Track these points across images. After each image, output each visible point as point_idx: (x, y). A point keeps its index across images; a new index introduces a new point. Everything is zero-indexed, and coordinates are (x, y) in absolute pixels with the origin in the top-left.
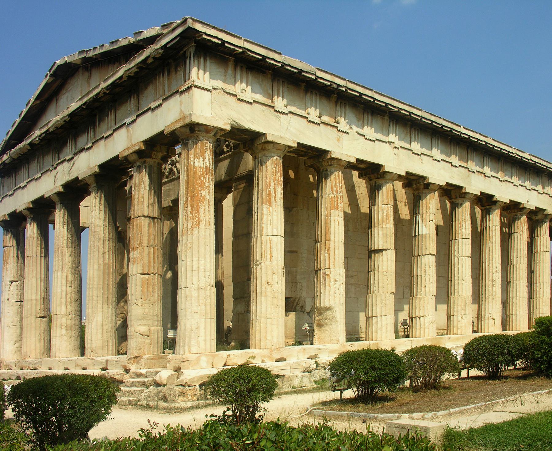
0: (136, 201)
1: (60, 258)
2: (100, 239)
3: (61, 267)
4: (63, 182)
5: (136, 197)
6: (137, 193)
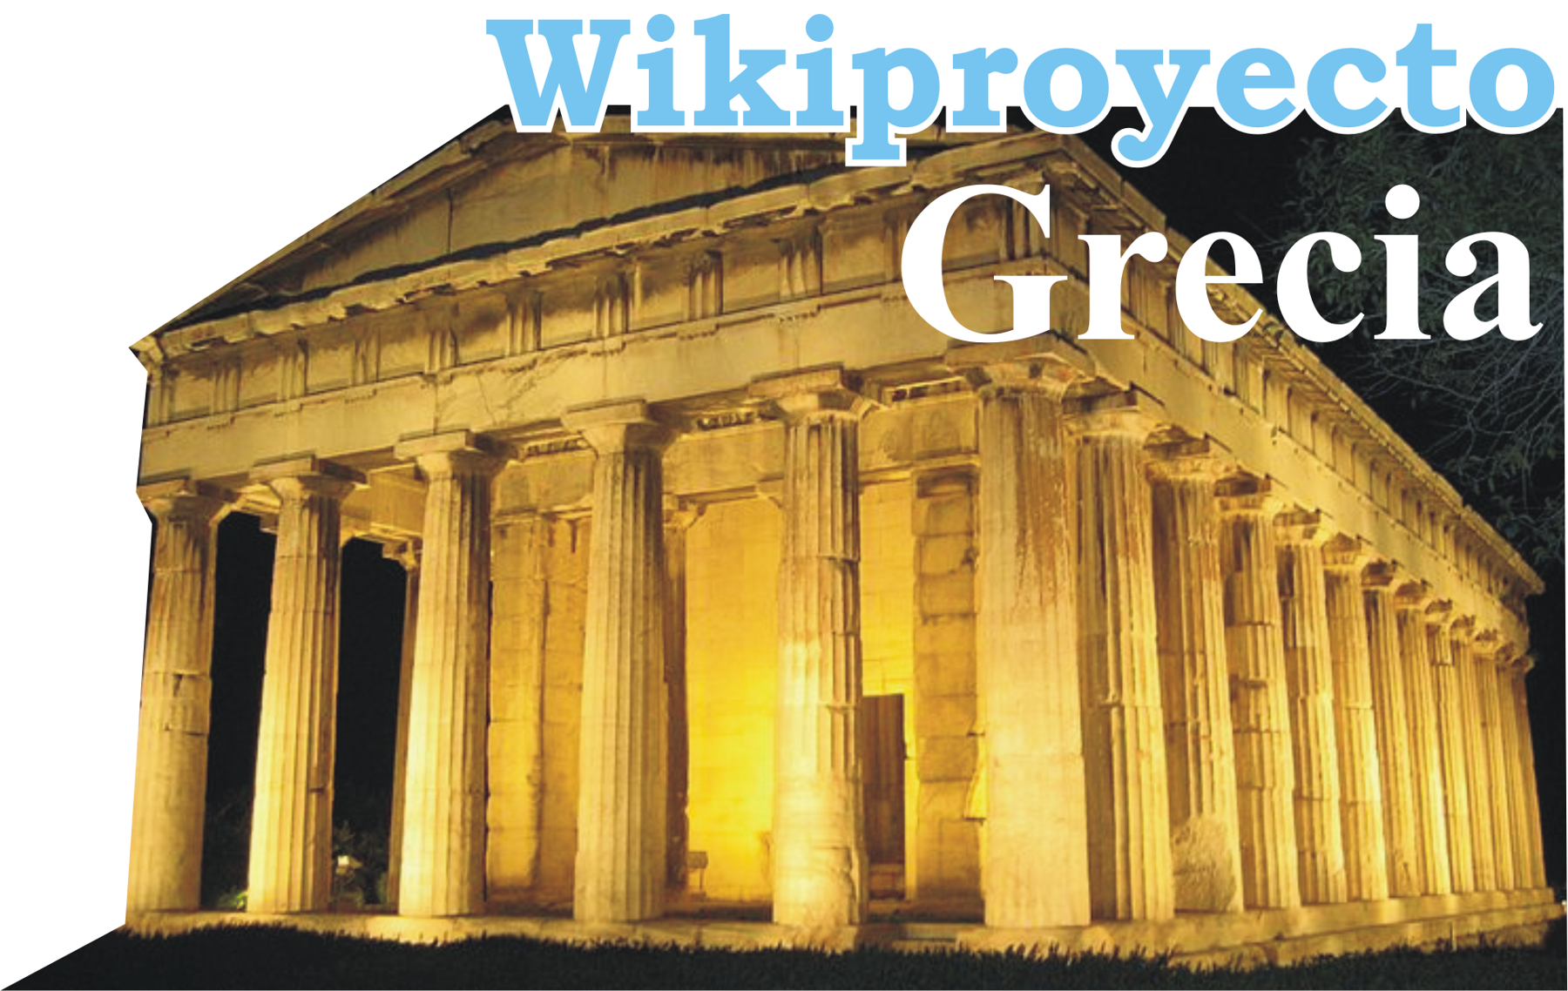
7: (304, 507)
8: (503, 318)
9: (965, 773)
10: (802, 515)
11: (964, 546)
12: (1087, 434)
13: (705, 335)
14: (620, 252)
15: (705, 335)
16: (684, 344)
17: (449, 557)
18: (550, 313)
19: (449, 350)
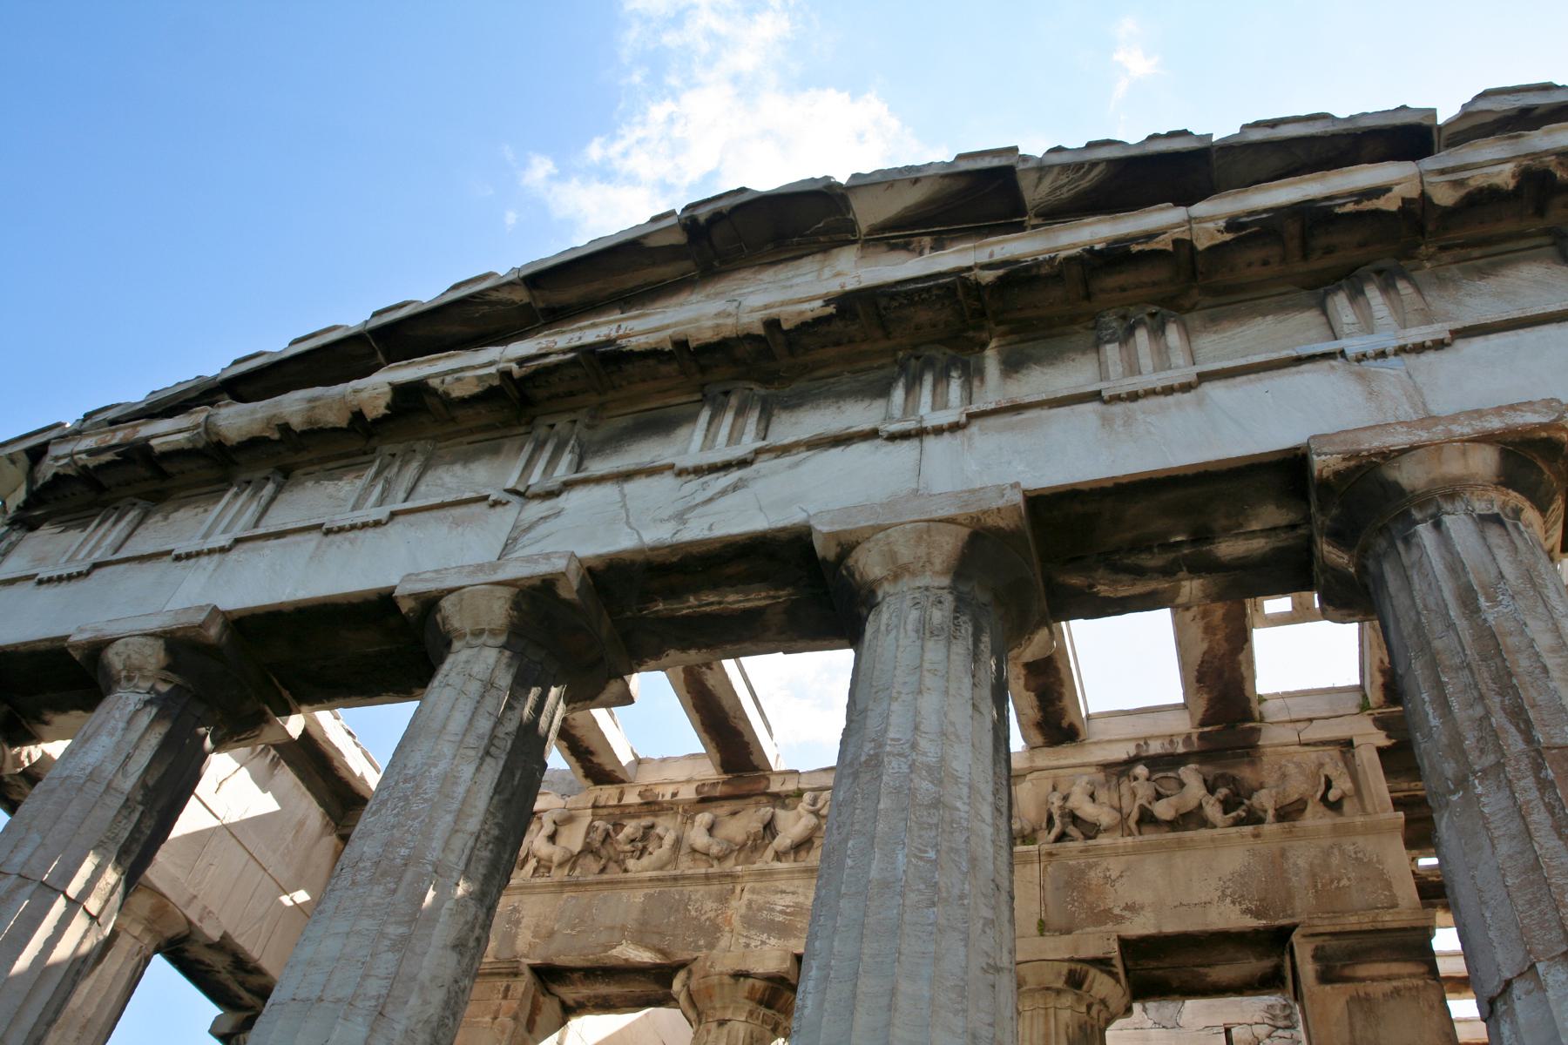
1: (394, 930)
2: (973, 861)
3: (374, 987)
8: (692, 418)
10: (1523, 663)
14: (988, 276)
15: (1168, 391)
16: (1118, 408)
17: (449, 779)
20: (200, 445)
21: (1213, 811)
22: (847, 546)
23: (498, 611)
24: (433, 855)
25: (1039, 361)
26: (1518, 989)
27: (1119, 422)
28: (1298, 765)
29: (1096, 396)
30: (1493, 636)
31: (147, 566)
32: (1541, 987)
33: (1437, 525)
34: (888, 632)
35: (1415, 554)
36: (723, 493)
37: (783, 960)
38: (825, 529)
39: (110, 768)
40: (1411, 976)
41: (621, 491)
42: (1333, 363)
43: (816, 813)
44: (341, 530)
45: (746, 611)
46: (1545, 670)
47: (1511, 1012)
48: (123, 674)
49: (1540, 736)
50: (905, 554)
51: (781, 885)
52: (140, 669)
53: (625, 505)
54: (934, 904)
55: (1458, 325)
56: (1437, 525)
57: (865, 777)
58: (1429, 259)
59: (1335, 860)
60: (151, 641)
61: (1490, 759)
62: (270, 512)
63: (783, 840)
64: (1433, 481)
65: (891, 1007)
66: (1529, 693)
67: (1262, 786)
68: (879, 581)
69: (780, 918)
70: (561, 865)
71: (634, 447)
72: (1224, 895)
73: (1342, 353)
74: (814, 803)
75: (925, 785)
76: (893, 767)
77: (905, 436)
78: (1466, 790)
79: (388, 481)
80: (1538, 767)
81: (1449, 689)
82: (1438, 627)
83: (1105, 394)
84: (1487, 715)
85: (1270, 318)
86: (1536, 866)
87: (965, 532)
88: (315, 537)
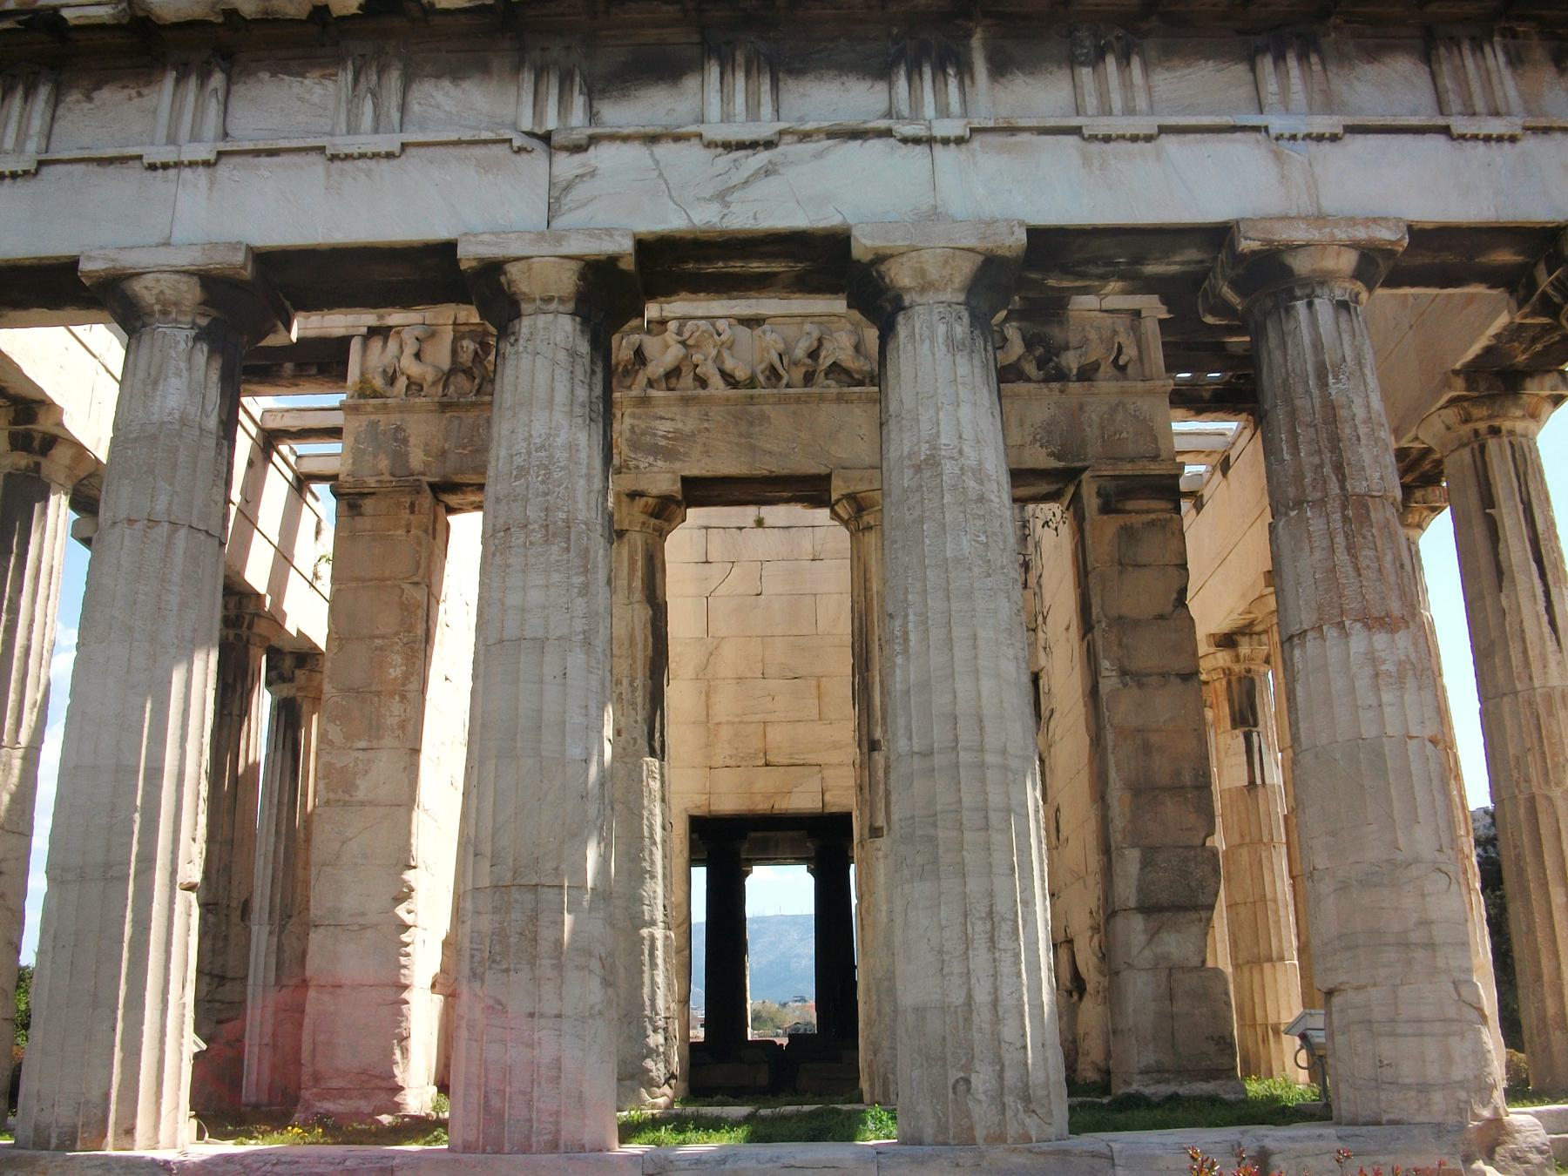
0: (1362, 430)
1: (578, 580)
3: (579, 625)
4: (671, 220)
5: (1360, 413)
6: (1358, 402)
7: (196, 339)
9: (1202, 899)
10: (1347, 431)
11: (1176, 586)
12: (1496, 423)
13: (1135, 139)
15: (1135, 139)
16: (1095, 147)
17: (572, 447)
18: (797, 72)
19: (579, 102)
20: (125, 21)
21: (1030, 368)
22: (881, 258)
23: (566, 281)
24: (582, 516)
25: (1021, 67)
26: (1310, 635)
27: (1096, 164)
28: (1098, 329)
29: (1077, 131)
30: (1334, 408)
31: (111, 169)
32: (1323, 637)
33: (1310, 305)
34: (922, 341)
35: (1292, 325)
36: (756, 174)
37: (674, 483)
38: (869, 243)
39: (193, 411)
40: (1163, 510)
41: (652, 154)
42: (1258, 136)
43: (683, 343)
44: (348, 157)
45: (761, 274)
46: (1359, 439)
47: (1303, 646)
48: (157, 308)
49: (1349, 487)
50: (933, 273)
51: (660, 412)
52: (176, 304)
53: (661, 174)
54: (989, 575)
55: (1350, 121)
56: (1310, 305)
57: (927, 474)
58: (1336, 27)
59: (1119, 416)
60: (185, 279)
61: (1319, 495)
62: (230, 109)
63: (656, 368)
64: (1314, 271)
65: (975, 647)
66: (1347, 455)
67: (1067, 348)
68: (909, 290)
69: (663, 443)
70: (434, 383)
71: (642, 93)
72: (1034, 440)
73: (1266, 129)
74: (679, 333)
75: (972, 484)
76: (949, 468)
77: (917, 141)
78: (1300, 510)
79: (374, 95)
80: (1344, 507)
81: (1301, 438)
82: (1300, 389)
83: (1086, 132)
84: (1321, 465)
85: (1211, 63)
86: (1333, 569)
87: (980, 259)
88: (317, 164)
